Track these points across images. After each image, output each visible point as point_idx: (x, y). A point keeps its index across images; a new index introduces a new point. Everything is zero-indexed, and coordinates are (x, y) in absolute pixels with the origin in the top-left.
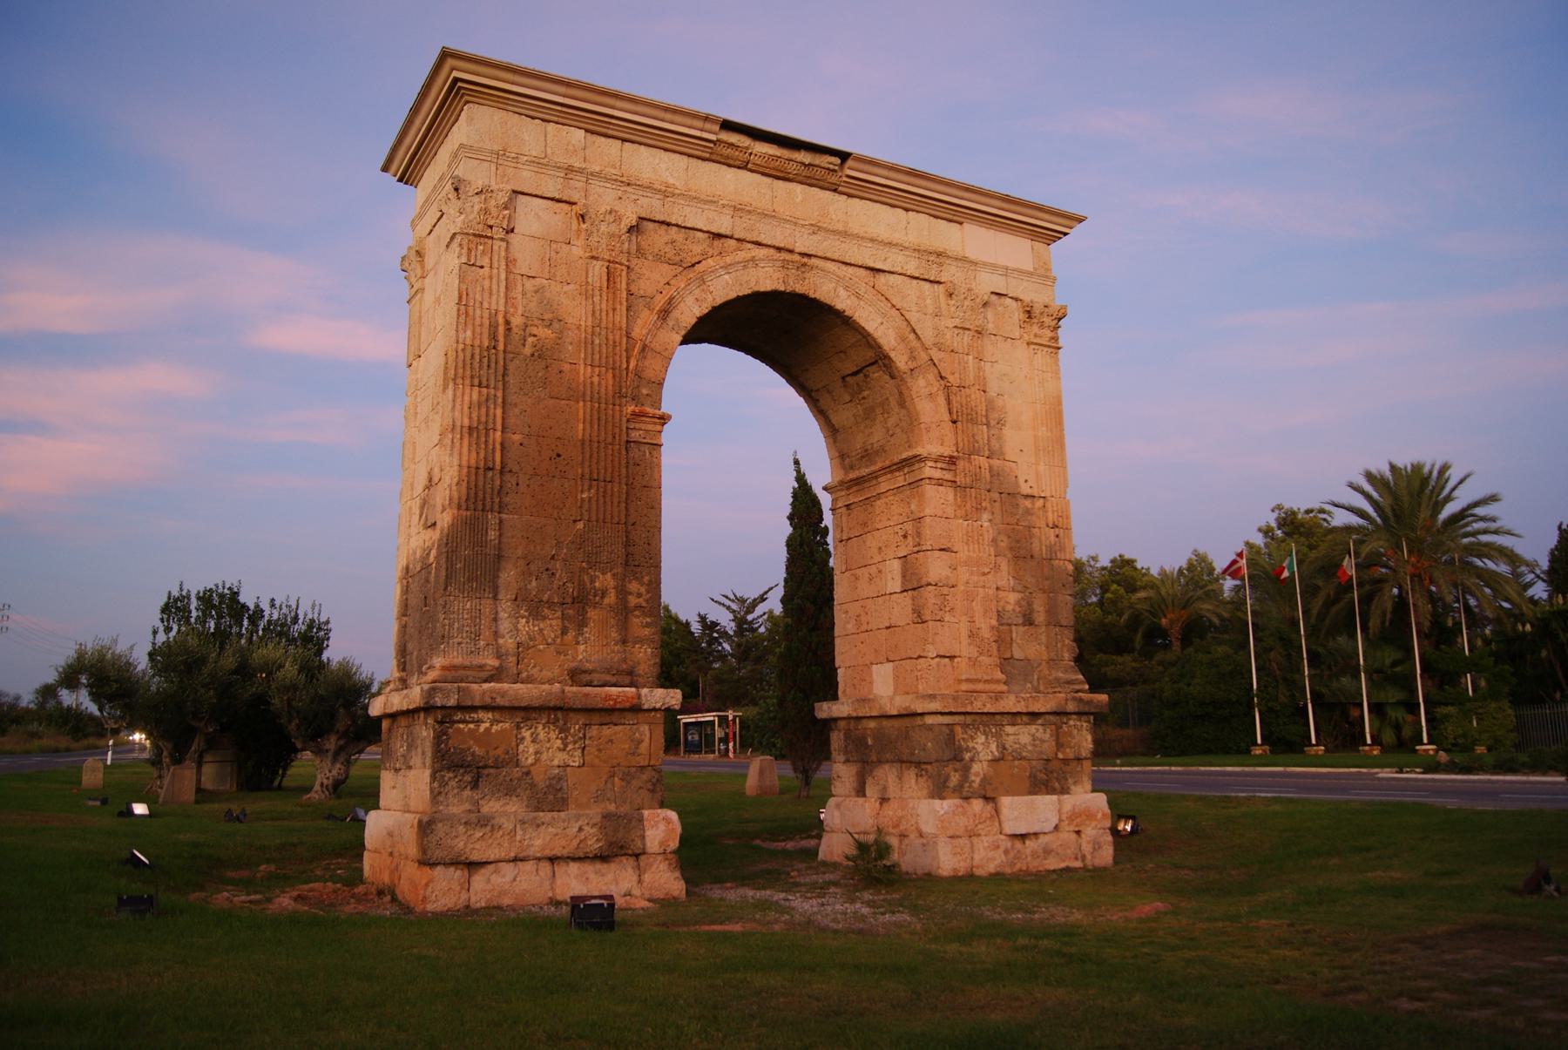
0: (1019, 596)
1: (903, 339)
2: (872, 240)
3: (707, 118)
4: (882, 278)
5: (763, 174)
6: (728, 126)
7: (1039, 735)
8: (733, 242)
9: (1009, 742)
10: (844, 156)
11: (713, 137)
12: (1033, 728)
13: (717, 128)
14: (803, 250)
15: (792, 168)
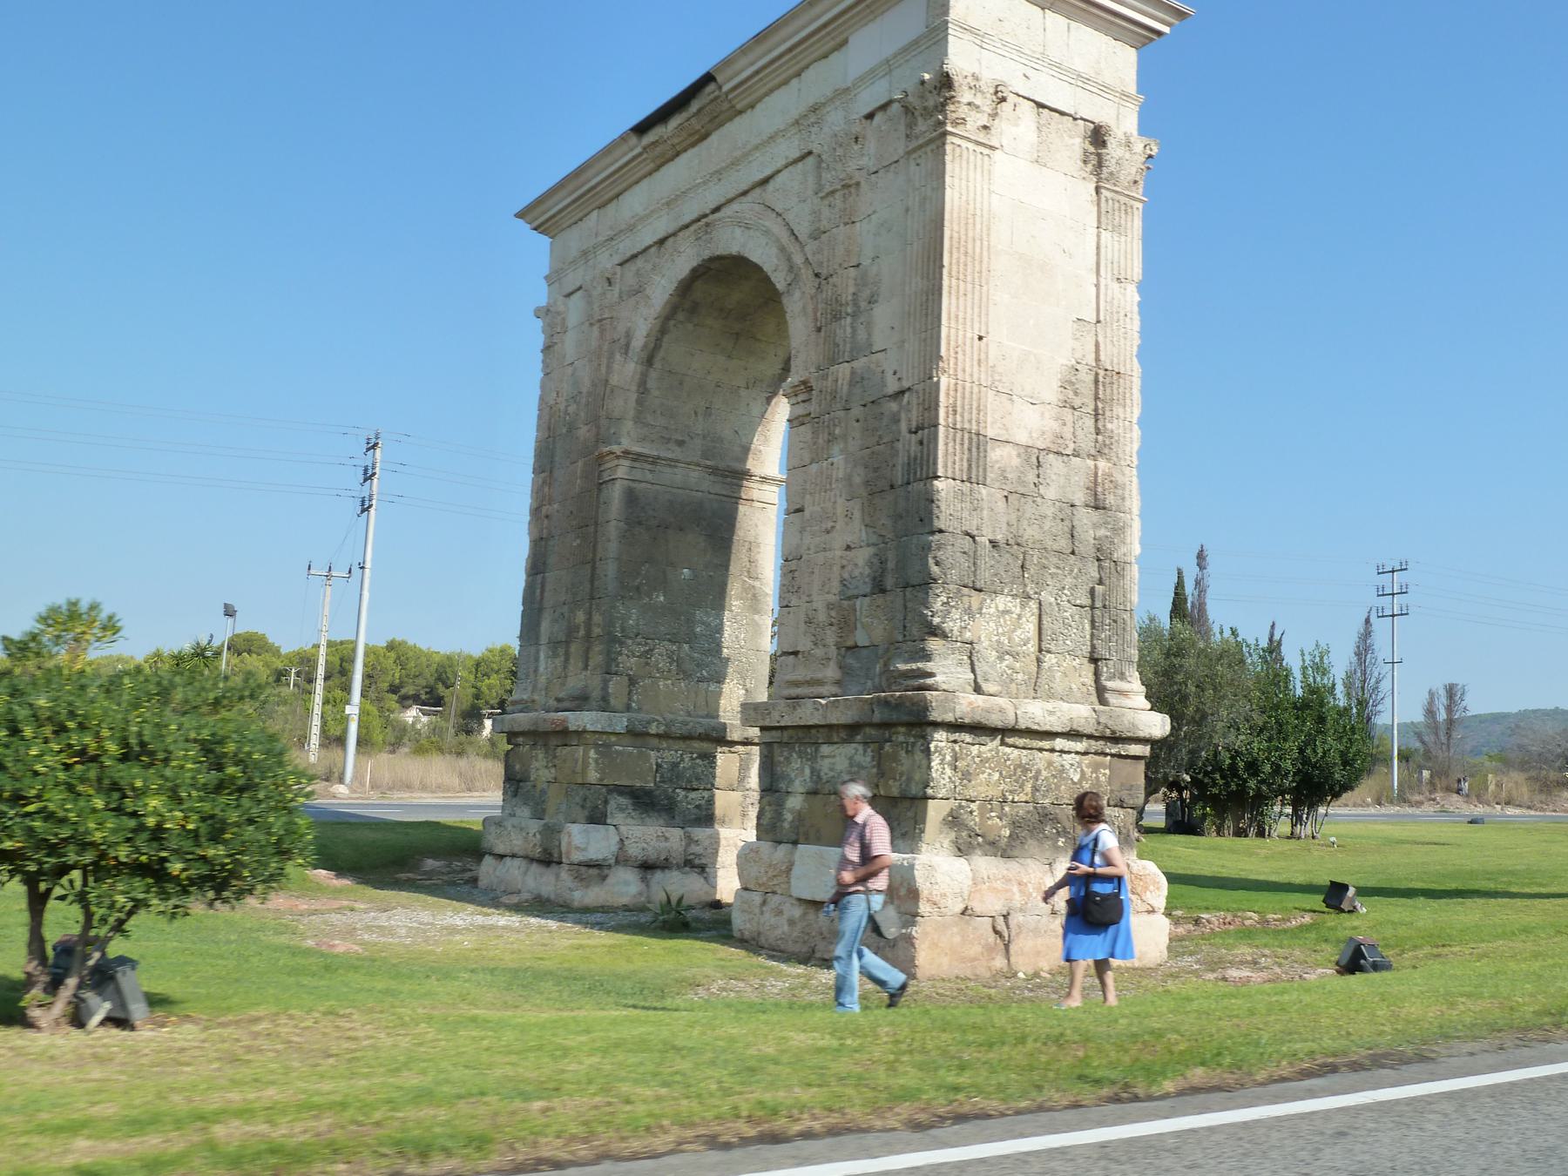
0: (871, 550)
1: (782, 249)
2: (756, 148)
3: (623, 138)
4: (771, 186)
5: (693, 145)
6: (641, 129)
7: (859, 758)
8: (671, 240)
9: (824, 765)
10: (708, 78)
11: (639, 150)
12: (849, 749)
13: (634, 140)
14: (713, 206)
15: (696, 124)
